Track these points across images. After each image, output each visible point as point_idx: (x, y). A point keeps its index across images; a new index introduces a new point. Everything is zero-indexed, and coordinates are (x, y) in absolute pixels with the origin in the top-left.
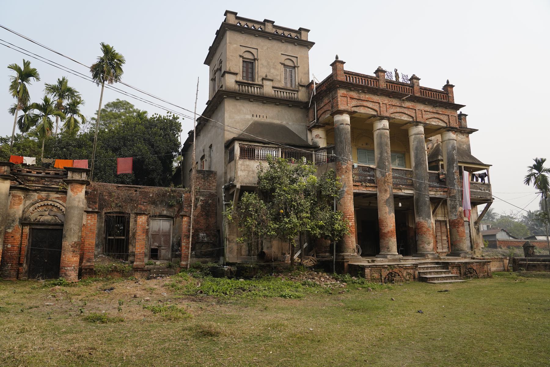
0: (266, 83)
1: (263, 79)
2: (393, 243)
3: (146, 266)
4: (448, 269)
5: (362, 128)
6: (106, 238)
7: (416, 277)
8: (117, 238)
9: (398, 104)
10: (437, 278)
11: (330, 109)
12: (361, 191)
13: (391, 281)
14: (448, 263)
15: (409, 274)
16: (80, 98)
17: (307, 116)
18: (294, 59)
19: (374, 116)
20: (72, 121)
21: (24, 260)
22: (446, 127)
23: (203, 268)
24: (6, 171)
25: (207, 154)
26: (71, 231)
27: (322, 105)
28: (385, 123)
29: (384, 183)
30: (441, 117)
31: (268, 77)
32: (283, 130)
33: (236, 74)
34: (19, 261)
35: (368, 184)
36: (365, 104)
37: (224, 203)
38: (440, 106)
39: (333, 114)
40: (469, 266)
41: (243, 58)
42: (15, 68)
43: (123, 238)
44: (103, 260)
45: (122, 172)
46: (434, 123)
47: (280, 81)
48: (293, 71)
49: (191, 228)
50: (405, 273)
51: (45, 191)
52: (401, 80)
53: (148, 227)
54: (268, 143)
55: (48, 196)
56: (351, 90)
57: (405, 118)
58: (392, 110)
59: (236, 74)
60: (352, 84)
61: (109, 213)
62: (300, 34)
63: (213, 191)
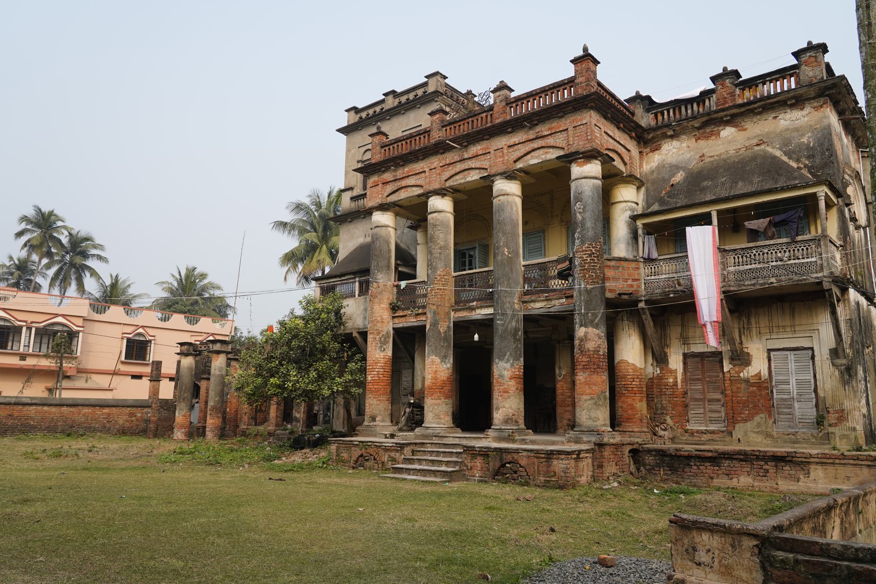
9: (457, 158)
10: (408, 471)
12: (410, 324)
30: (550, 141)
33: (351, 189)
36: (404, 183)
46: (534, 162)
50: (387, 456)
54: (344, 275)
56: (384, 172)
57: (474, 176)
59: (351, 189)
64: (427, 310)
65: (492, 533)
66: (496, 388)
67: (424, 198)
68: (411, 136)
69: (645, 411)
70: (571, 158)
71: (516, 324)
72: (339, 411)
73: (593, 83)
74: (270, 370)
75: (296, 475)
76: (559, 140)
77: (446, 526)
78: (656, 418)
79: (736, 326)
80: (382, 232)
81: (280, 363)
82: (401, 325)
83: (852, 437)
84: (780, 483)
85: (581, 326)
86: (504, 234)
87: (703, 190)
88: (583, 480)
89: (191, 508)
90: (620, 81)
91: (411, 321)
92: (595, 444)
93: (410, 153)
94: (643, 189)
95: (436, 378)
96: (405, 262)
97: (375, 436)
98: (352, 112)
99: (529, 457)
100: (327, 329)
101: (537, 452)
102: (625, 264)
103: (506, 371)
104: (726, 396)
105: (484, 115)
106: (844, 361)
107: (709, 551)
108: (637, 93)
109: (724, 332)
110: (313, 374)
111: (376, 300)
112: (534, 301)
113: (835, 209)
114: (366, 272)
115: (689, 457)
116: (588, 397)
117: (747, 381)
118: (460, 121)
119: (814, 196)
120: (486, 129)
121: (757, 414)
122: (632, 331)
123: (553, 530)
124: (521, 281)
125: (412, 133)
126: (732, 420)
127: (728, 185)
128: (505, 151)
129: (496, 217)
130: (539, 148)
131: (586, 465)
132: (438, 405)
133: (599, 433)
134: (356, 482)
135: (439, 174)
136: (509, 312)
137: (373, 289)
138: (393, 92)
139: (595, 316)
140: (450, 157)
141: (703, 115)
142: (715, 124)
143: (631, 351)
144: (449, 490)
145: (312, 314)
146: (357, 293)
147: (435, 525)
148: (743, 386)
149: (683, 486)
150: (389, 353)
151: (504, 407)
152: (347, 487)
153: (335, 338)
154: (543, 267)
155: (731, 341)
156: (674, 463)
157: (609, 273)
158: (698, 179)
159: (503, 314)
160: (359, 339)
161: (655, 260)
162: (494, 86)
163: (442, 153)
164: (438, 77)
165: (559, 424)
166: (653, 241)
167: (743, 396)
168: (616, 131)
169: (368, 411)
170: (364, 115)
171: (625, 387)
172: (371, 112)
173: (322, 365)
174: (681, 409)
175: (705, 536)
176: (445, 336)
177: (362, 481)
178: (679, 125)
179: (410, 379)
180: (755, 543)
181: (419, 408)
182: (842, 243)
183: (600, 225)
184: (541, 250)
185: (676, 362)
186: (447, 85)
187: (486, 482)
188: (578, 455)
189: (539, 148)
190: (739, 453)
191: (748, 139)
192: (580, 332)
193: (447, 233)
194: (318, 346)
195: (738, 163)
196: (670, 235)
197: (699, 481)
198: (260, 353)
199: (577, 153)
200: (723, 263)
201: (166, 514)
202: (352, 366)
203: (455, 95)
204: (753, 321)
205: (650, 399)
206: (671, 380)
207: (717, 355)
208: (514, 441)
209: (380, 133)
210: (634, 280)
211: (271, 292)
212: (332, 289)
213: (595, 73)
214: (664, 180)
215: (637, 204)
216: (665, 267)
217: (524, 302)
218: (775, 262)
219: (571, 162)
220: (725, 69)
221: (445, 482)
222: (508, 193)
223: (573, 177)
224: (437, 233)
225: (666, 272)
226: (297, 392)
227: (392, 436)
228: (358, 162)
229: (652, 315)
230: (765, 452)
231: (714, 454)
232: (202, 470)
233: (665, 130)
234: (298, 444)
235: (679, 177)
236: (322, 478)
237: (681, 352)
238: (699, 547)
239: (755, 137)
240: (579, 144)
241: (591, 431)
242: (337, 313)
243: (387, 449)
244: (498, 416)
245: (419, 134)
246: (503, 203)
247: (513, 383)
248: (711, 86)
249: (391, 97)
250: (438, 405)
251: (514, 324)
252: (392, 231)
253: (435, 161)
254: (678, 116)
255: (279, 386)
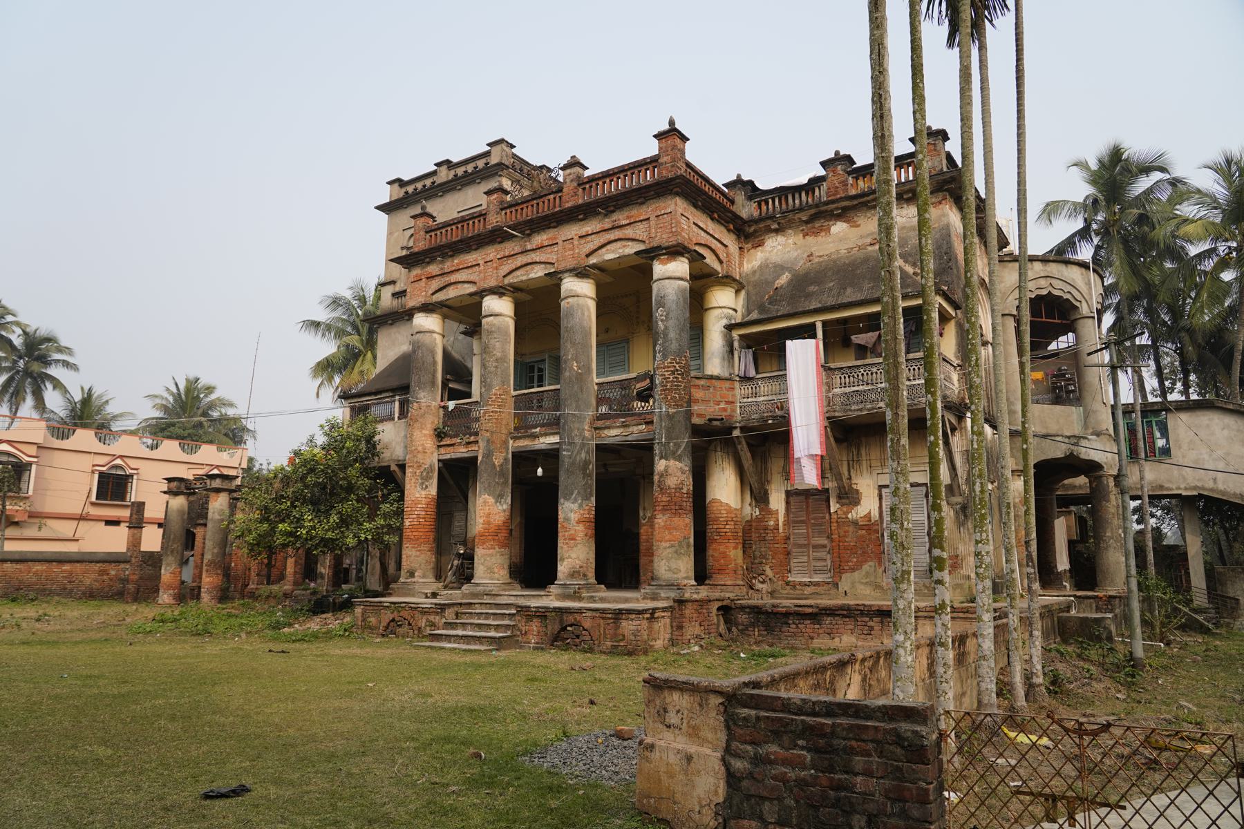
9: (518, 249)
10: (448, 638)
12: (459, 455)
30: (629, 232)
33: (393, 282)
36: (453, 278)
40: (570, 619)
46: (611, 256)
54: (380, 392)
56: (428, 263)
57: (538, 272)
59: (393, 282)
64: (480, 438)
65: (517, 708)
66: (560, 534)
67: (477, 298)
68: (463, 220)
69: (740, 561)
70: (652, 253)
71: (587, 456)
72: (374, 565)
73: (681, 164)
74: (278, 514)
75: (305, 646)
76: (639, 231)
77: (464, 700)
78: (752, 570)
79: (845, 458)
80: (426, 338)
81: (292, 503)
82: (448, 457)
83: (966, 586)
84: (885, 642)
85: (661, 458)
86: (573, 344)
87: (809, 296)
88: (659, 644)
89: (151, 689)
90: (716, 162)
91: (461, 452)
92: (675, 601)
93: (461, 241)
94: (743, 293)
95: (489, 523)
96: (457, 376)
97: (413, 596)
98: (396, 185)
99: (594, 618)
100: (355, 461)
101: (603, 611)
102: (716, 383)
103: (574, 513)
104: (832, 541)
105: (552, 197)
106: (959, 499)
107: (678, 711)
108: (739, 176)
109: (826, 466)
110: (334, 518)
111: (417, 425)
112: (608, 428)
113: (953, 323)
114: (404, 389)
115: (787, 615)
116: (667, 544)
117: (855, 523)
118: (523, 203)
119: (904, 309)
120: (553, 214)
121: (866, 561)
122: (726, 465)
123: (592, 702)
124: (594, 402)
125: (474, 214)
126: (838, 569)
127: (835, 291)
128: (576, 242)
129: (564, 323)
130: (616, 241)
131: (663, 626)
132: (491, 555)
133: (679, 587)
134: (380, 653)
135: (497, 268)
136: (578, 441)
137: (413, 410)
138: (447, 162)
139: (677, 445)
140: (510, 247)
141: (809, 207)
142: (824, 218)
143: (725, 488)
144: (492, 660)
145: (335, 444)
146: (396, 415)
147: (452, 700)
148: (851, 529)
149: (776, 649)
150: (433, 491)
151: (570, 557)
152: (365, 658)
153: (365, 472)
154: (624, 385)
155: (839, 477)
156: (771, 621)
157: (698, 394)
158: (804, 282)
159: (570, 444)
160: (399, 473)
161: (753, 379)
162: (564, 162)
163: (500, 242)
164: (504, 146)
165: (642, 578)
166: (750, 357)
167: (851, 540)
168: (709, 222)
169: (405, 564)
170: (410, 189)
171: (718, 531)
172: (419, 185)
173: (346, 507)
174: (782, 557)
175: (676, 696)
176: (501, 470)
177: (389, 651)
178: (784, 217)
179: (463, 523)
180: (721, 700)
181: (469, 558)
182: (959, 362)
183: (686, 336)
184: (624, 365)
185: (777, 501)
186: (514, 156)
187: (542, 649)
188: (653, 614)
189: (616, 241)
190: (842, 608)
191: (861, 237)
192: (660, 465)
193: (507, 342)
194: (345, 480)
195: (849, 265)
196: (766, 349)
197: (797, 642)
198: (267, 492)
199: (659, 248)
200: (827, 384)
201: (114, 697)
202: (386, 507)
203: (526, 169)
204: (863, 452)
205: (746, 546)
206: (772, 523)
207: (823, 494)
208: (580, 599)
209: (425, 214)
210: (727, 403)
211: (281, 413)
212: (366, 408)
213: (683, 152)
214: (769, 283)
215: (735, 311)
216: (764, 388)
217: (596, 429)
218: (867, 388)
219: (652, 259)
220: (837, 153)
221: (491, 650)
222: (580, 294)
223: (655, 277)
224: (492, 341)
225: (765, 392)
226: (314, 540)
227: (434, 595)
228: (402, 248)
229: (748, 444)
230: (871, 606)
231: (815, 610)
232: (185, 641)
233: (769, 222)
234: (319, 607)
235: (784, 279)
236: (336, 649)
237: (783, 489)
238: (670, 708)
239: (868, 235)
240: (663, 238)
241: (670, 585)
242: (369, 440)
243: (424, 612)
244: (563, 568)
245: (472, 217)
246: (572, 306)
247: (581, 527)
248: (822, 172)
249: (444, 168)
250: (491, 555)
251: (583, 455)
252: (438, 338)
253: (492, 252)
254: (784, 206)
255: (290, 534)
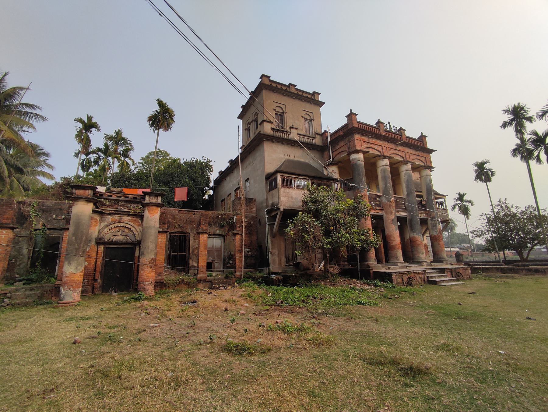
0: (292, 130)
1: (291, 128)
2: (400, 253)
3: (208, 278)
4: (444, 273)
5: (371, 164)
6: (170, 254)
7: (426, 280)
8: (179, 254)
11: (347, 149)
13: (410, 284)
14: (444, 269)
15: (421, 278)
16: (132, 146)
17: (323, 157)
18: (311, 114)
19: (379, 156)
20: (125, 163)
21: (98, 276)
22: (425, 166)
23: (255, 277)
24: (90, 195)
25: (242, 186)
26: (149, 248)
27: (338, 147)
28: (386, 162)
29: (390, 207)
31: (294, 127)
32: (308, 165)
34: (94, 277)
35: (377, 208)
37: (267, 223)
38: (420, 151)
39: (349, 154)
41: (276, 111)
42: (80, 121)
43: (184, 253)
44: (170, 274)
45: (178, 200)
47: (302, 130)
48: (310, 123)
49: (243, 244)
51: (118, 214)
52: (393, 130)
53: (206, 244)
54: (302, 175)
55: (121, 219)
56: (363, 135)
57: (398, 158)
58: (390, 152)
60: (365, 130)
61: (172, 233)
62: (314, 96)
63: (254, 215)
